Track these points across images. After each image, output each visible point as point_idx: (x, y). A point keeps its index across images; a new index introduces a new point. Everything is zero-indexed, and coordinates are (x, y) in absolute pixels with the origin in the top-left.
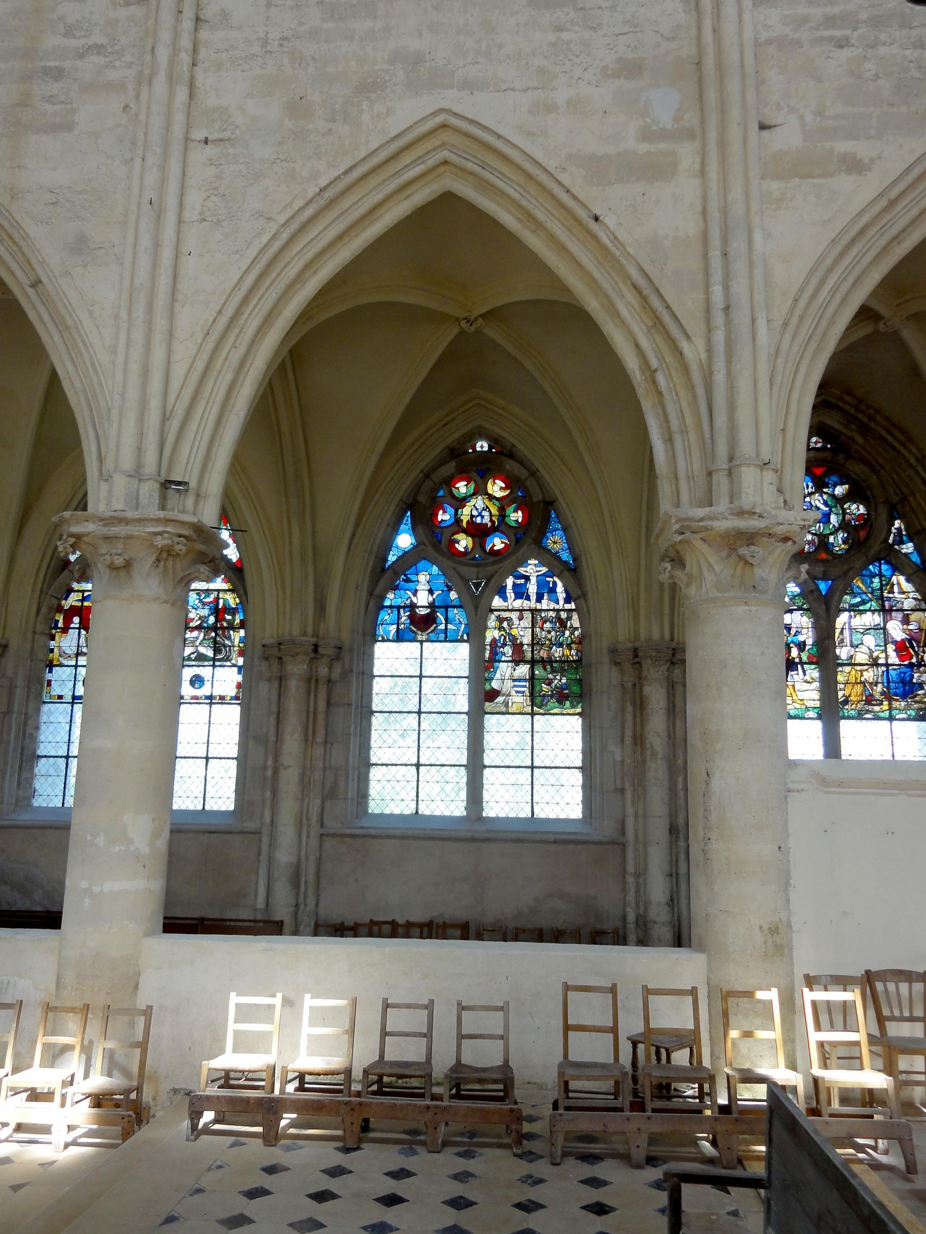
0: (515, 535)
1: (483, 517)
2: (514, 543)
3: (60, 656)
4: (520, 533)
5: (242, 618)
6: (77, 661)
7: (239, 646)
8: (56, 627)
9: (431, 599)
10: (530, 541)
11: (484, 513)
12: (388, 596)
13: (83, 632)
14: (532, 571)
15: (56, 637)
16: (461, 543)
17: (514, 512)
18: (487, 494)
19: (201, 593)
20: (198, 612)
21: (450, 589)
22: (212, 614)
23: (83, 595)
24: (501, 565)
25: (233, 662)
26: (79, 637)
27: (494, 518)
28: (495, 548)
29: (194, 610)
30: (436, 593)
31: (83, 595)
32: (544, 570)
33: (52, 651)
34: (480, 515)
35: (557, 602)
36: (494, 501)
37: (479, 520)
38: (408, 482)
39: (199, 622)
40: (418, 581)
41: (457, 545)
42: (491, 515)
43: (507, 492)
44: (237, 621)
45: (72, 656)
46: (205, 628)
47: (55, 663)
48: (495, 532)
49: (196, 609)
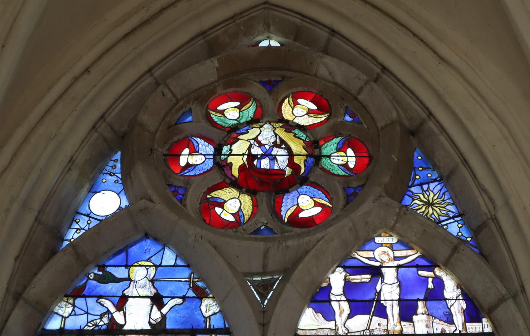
0: (344, 189)
1: (273, 158)
2: (342, 203)
4: (355, 184)
9: (156, 315)
10: (378, 190)
11: (275, 151)
12: (57, 309)
14: (385, 258)
16: (227, 205)
17: (338, 150)
18: (282, 120)
21: (201, 295)
24: (319, 235)
27: (296, 160)
28: (302, 215)
30: (172, 303)
32: (412, 255)
34: (267, 154)
35: (449, 319)
36: (297, 131)
37: (265, 164)
38: (119, 87)
40: (129, 279)
41: (218, 210)
42: (291, 154)
43: (322, 118)
48: (301, 185)
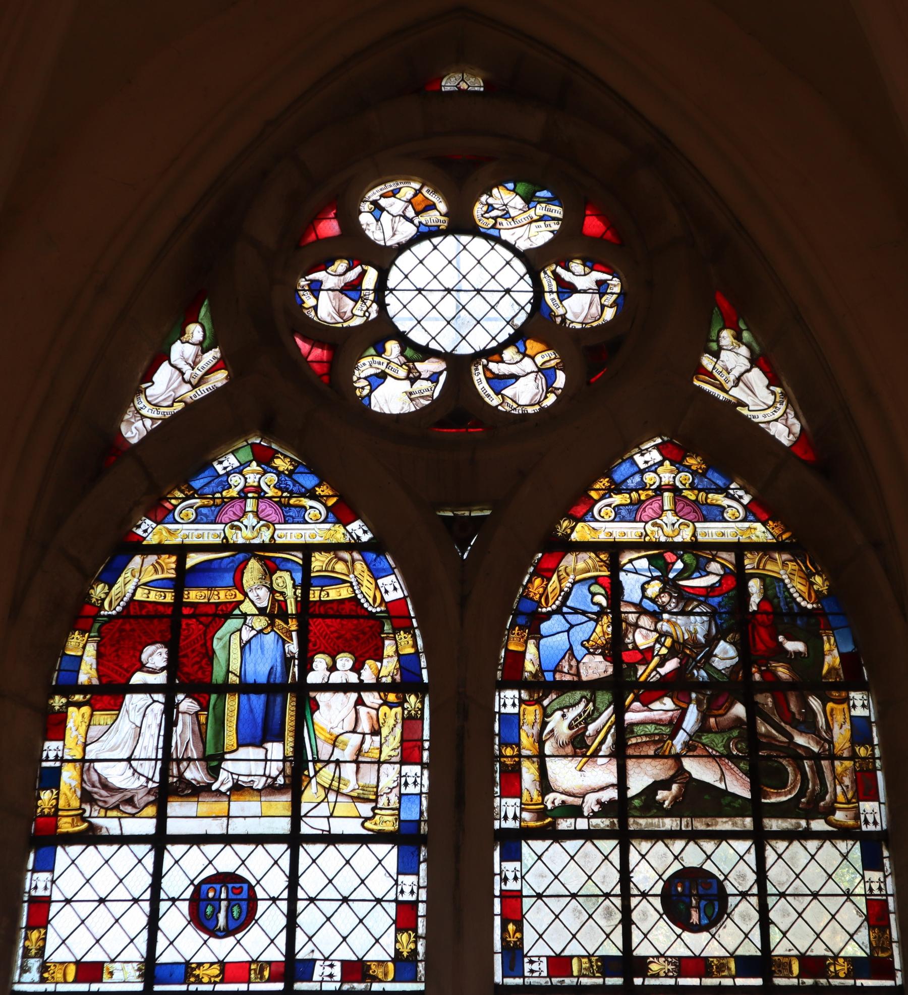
3: (87, 797)
5: (849, 648)
6: (162, 818)
7: (853, 756)
8: (70, 688)
13: (187, 704)
15: (70, 724)
19: (670, 557)
20: (665, 627)
22: (722, 635)
23: (181, 562)
25: (839, 816)
26: (170, 723)
29: (645, 621)
31: (181, 562)
33: (52, 779)
39: (672, 665)
44: (832, 660)
45: (141, 798)
46: (700, 686)
47: (66, 825)
49: (656, 616)
